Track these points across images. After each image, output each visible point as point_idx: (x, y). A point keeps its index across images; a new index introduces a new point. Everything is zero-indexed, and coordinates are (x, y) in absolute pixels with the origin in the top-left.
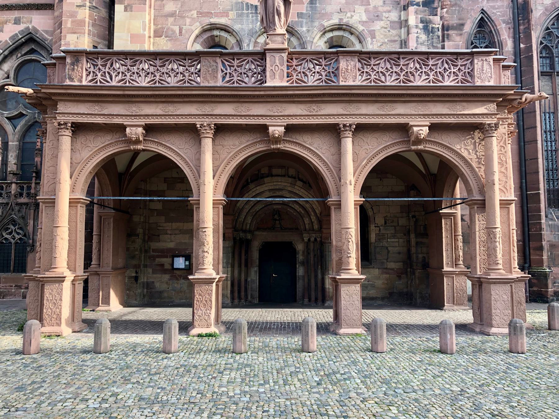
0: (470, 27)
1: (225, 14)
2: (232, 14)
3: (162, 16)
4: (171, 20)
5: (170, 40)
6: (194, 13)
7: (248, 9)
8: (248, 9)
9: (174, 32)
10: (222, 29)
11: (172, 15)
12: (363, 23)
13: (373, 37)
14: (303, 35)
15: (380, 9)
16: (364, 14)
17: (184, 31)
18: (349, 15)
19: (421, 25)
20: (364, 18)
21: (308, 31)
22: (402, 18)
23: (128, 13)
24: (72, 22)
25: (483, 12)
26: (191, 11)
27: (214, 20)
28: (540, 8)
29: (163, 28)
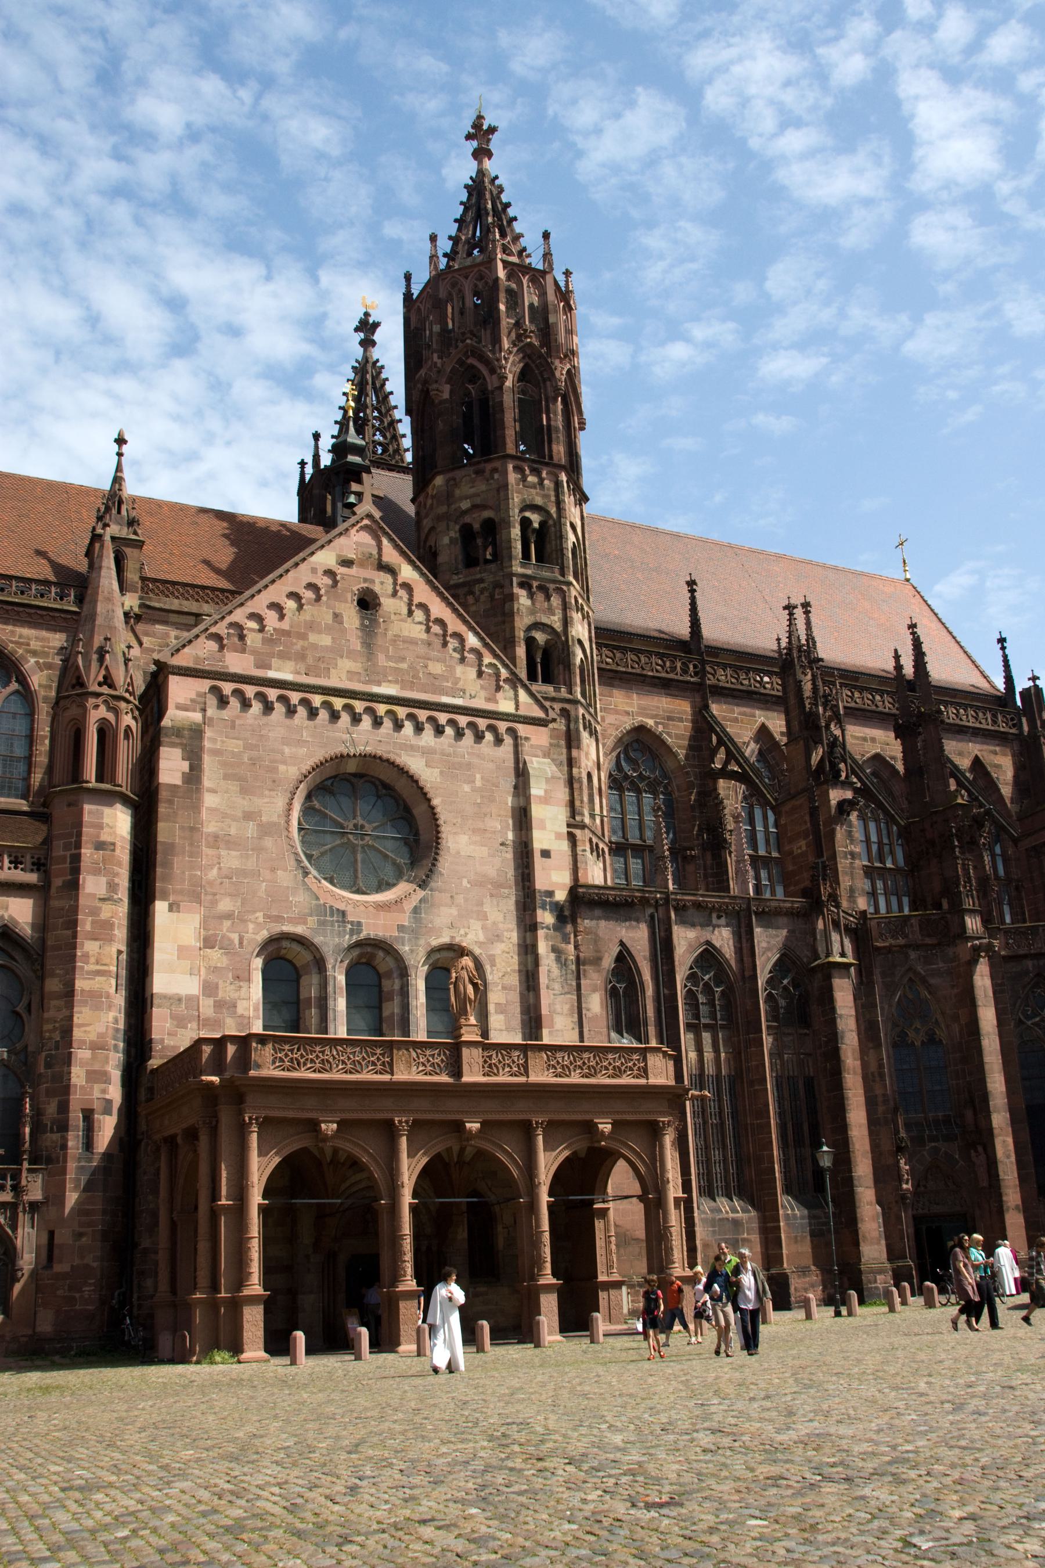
0: (608, 962)
1: (302, 920)
2: (312, 921)
3: (214, 917)
4: (227, 924)
5: (226, 954)
6: (260, 915)
7: (332, 915)
8: (332, 915)
9: (231, 941)
10: (294, 940)
11: (229, 916)
12: (481, 944)
13: (493, 965)
14: (406, 957)
15: (501, 926)
16: (480, 932)
17: (245, 942)
18: (462, 932)
19: (552, 956)
20: (481, 938)
21: (412, 951)
22: (528, 942)
23: (174, 915)
24: (93, 922)
25: (622, 943)
26: (255, 912)
27: (288, 928)
28: (683, 942)
29: (216, 935)
